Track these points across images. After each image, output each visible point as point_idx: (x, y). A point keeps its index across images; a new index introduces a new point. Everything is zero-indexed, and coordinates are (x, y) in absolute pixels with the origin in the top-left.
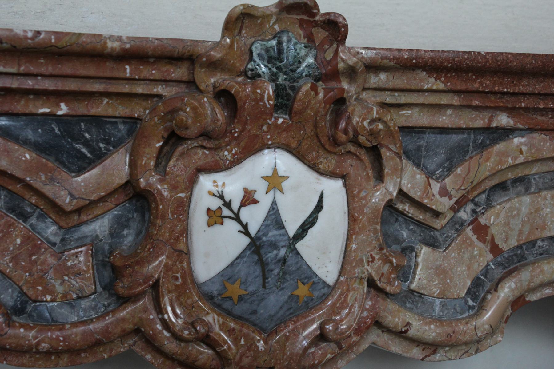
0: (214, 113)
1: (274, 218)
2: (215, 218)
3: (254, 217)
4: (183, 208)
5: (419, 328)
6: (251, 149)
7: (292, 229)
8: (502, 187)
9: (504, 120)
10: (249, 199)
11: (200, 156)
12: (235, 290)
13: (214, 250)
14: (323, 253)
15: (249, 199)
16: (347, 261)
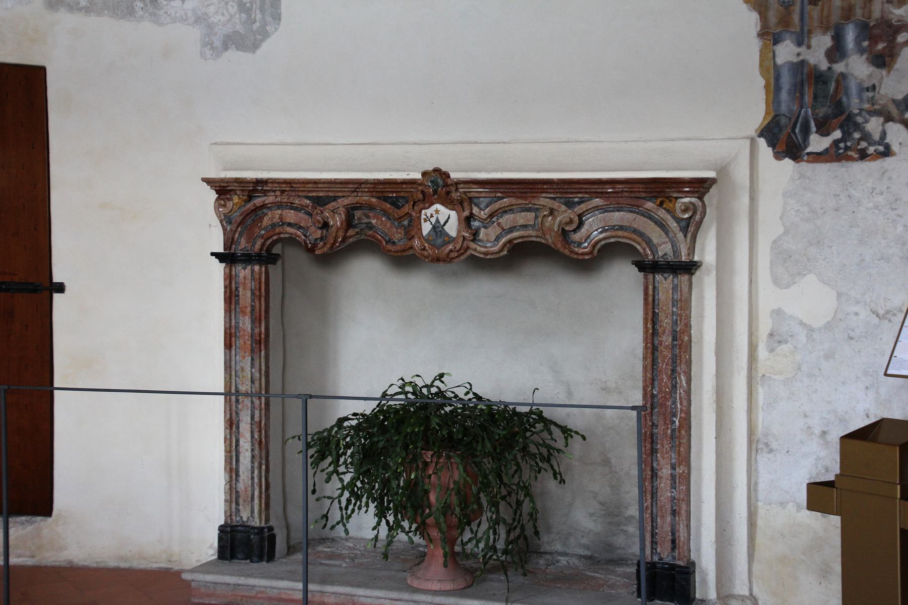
0: (421, 196)
1: (438, 221)
2: (425, 221)
3: (433, 220)
4: (419, 218)
5: (478, 248)
6: (432, 204)
7: (442, 223)
8: (505, 212)
9: (499, 195)
10: (432, 216)
11: (421, 205)
12: (431, 238)
13: (426, 228)
14: (452, 229)
15: (432, 216)
16: (459, 232)
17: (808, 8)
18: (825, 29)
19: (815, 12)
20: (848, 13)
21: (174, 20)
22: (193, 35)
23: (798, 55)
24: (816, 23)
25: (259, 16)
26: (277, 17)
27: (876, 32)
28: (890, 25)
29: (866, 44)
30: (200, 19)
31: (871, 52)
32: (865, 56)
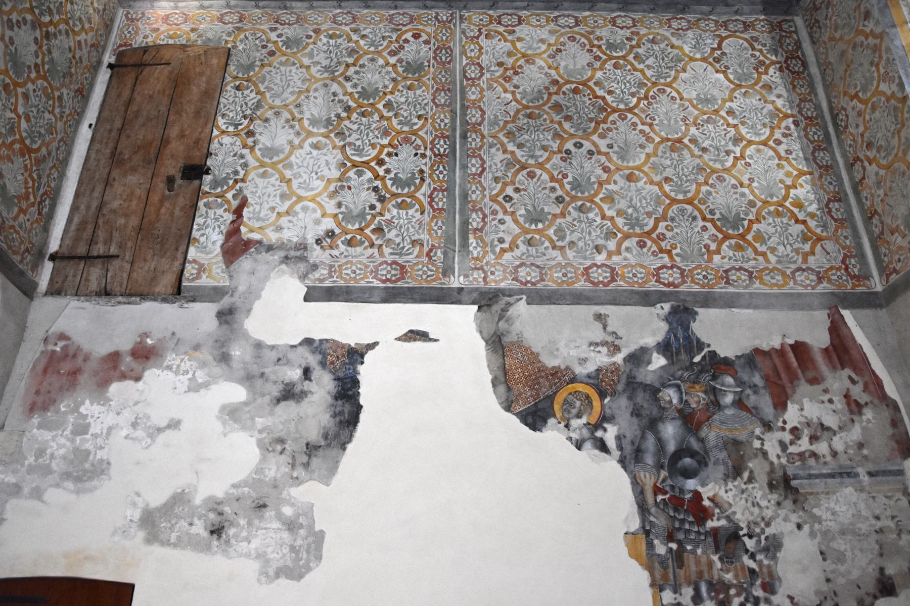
17: (677, 570)
18: (689, 584)
19: (681, 573)
20: (700, 574)
21: (240, 555)
22: (253, 566)
23: (675, 599)
24: (683, 580)
25: (305, 556)
26: (319, 558)
27: (718, 587)
28: (725, 584)
29: (713, 594)
30: (260, 556)
31: (717, 599)
32: (714, 602)
